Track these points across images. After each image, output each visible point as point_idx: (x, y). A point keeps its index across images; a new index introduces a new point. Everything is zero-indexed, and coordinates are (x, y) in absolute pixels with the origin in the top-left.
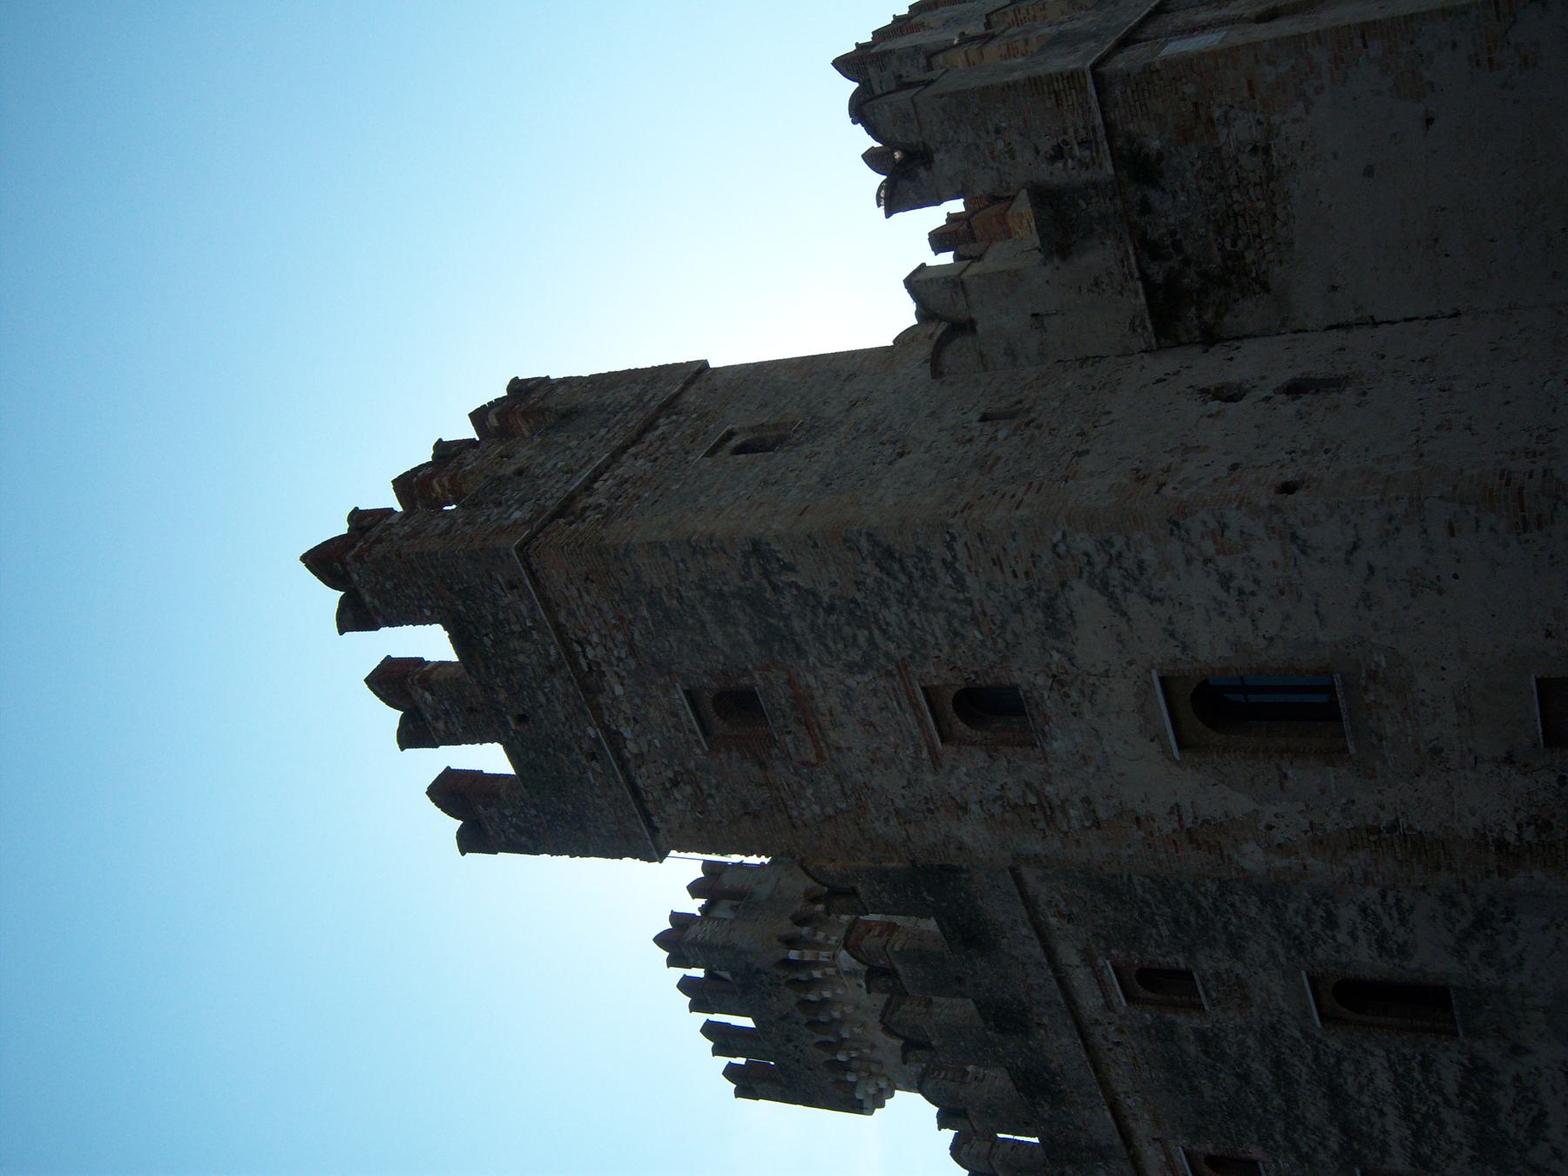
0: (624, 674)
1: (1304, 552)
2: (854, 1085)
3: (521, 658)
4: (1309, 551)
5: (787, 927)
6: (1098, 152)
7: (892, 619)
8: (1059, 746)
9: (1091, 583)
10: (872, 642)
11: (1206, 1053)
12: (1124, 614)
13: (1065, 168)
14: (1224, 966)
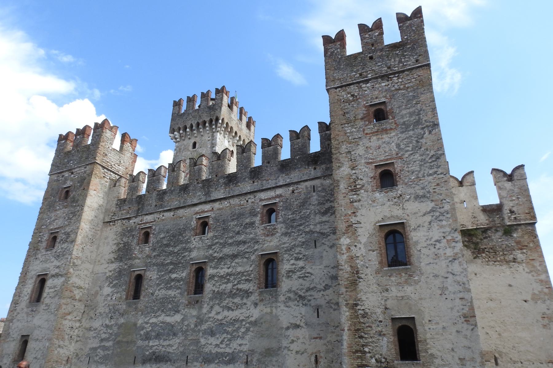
0: (389, 86)
1: (450, 261)
3: (393, 60)
4: (451, 263)
5: (226, 121)
7: (416, 157)
8: (377, 195)
9: (433, 208)
10: (407, 151)
11: (247, 224)
12: (424, 215)
14: (279, 231)
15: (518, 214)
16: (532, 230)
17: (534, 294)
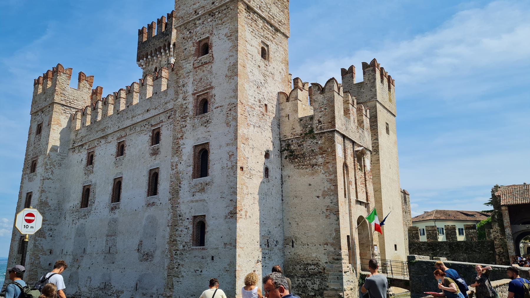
2: (143, 59)
6: (319, 130)
13: (317, 123)
15: (323, 124)
16: (332, 137)
17: (324, 191)
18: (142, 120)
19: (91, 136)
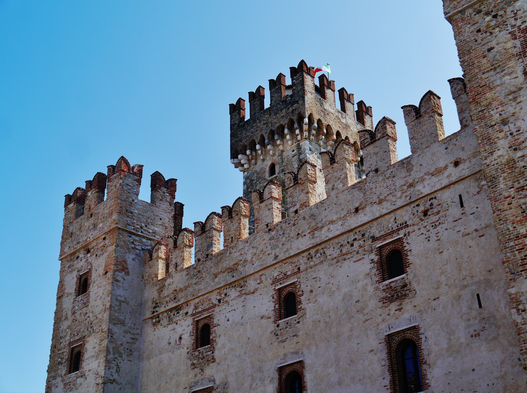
2: (245, 154)
5: (316, 117)
18: (343, 231)
19: (202, 286)
